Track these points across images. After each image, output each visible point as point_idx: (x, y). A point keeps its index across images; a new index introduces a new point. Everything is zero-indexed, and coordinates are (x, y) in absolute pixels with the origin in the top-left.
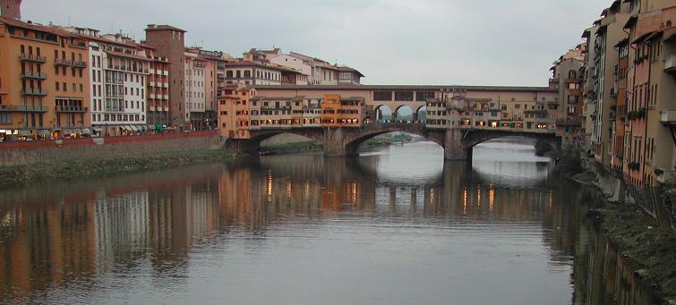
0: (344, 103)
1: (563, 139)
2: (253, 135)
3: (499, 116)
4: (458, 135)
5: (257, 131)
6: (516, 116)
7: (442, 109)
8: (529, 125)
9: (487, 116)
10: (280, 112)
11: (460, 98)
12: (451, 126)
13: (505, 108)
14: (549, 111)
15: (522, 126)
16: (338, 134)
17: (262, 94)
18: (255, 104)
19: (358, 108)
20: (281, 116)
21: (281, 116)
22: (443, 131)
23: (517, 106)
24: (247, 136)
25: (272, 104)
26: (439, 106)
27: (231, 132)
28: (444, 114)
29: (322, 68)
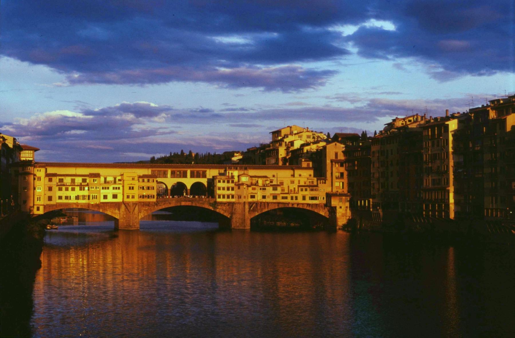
1: (337, 208)
2: (47, 210)
3: (279, 190)
4: (247, 207)
5: (52, 206)
6: (291, 191)
7: (231, 185)
8: (304, 198)
9: (270, 190)
10: (77, 188)
12: (242, 200)
13: (282, 184)
15: (296, 198)
18: (50, 180)
21: (78, 192)
23: (292, 182)
26: (228, 182)
28: (233, 189)
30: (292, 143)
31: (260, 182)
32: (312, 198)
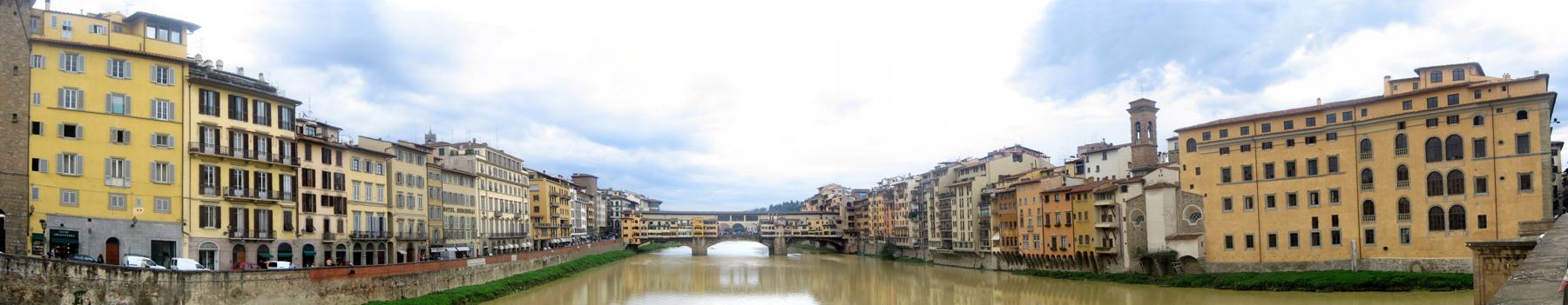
0: (706, 222)
3: (807, 229)
4: (783, 240)
10: (662, 228)
11: (782, 219)
12: (779, 235)
13: (810, 224)
14: (838, 225)
16: (703, 241)
17: (645, 216)
18: (644, 223)
19: (716, 225)
20: (662, 230)
22: (773, 239)
23: (818, 223)
24: (638, 242)
25: (656, 223)
27: (630, 241)
28: (773, 228)
29: (645, 201)
30: (826, 196)
31: (794, 224)
32: (832, 233)
